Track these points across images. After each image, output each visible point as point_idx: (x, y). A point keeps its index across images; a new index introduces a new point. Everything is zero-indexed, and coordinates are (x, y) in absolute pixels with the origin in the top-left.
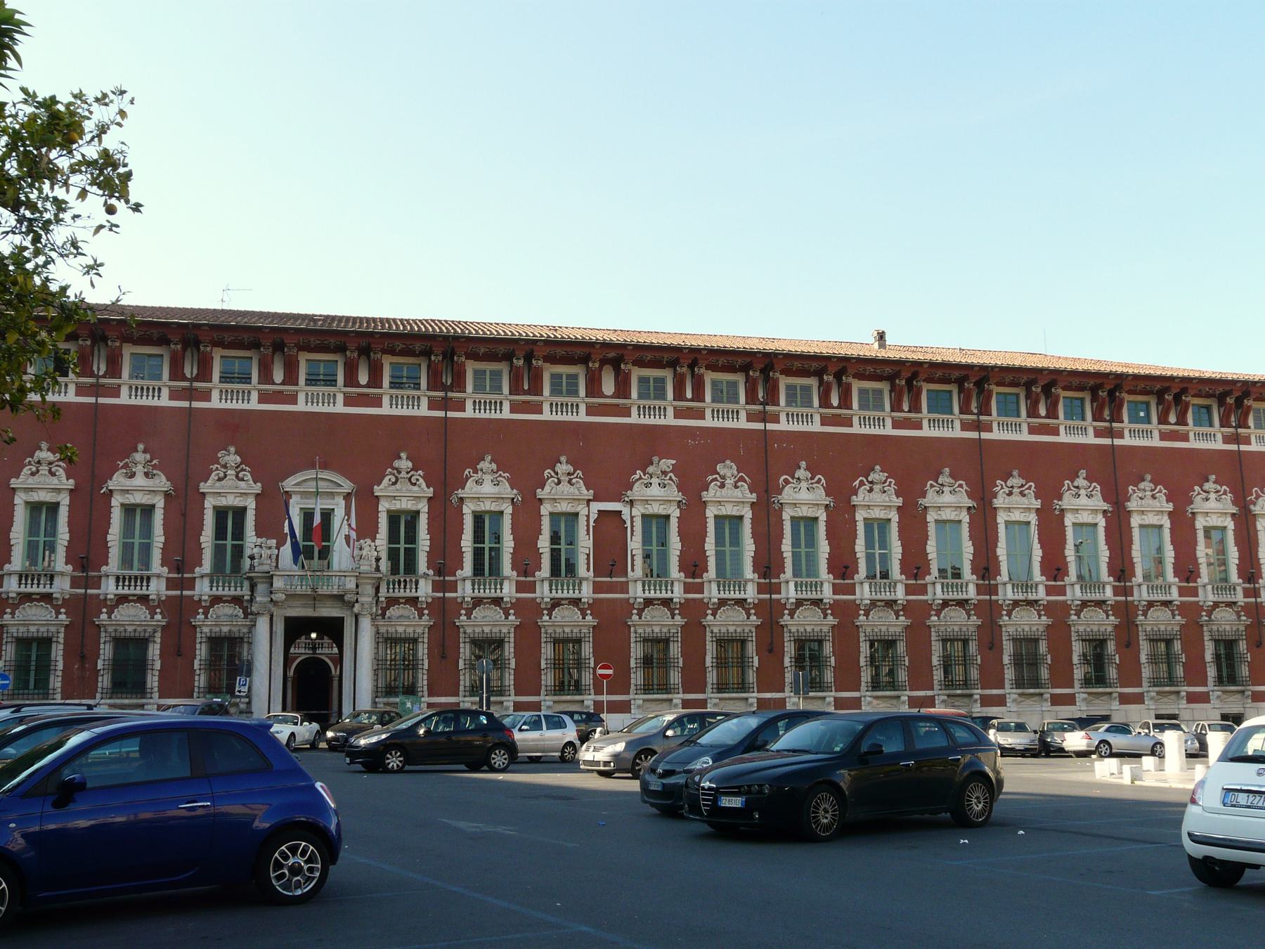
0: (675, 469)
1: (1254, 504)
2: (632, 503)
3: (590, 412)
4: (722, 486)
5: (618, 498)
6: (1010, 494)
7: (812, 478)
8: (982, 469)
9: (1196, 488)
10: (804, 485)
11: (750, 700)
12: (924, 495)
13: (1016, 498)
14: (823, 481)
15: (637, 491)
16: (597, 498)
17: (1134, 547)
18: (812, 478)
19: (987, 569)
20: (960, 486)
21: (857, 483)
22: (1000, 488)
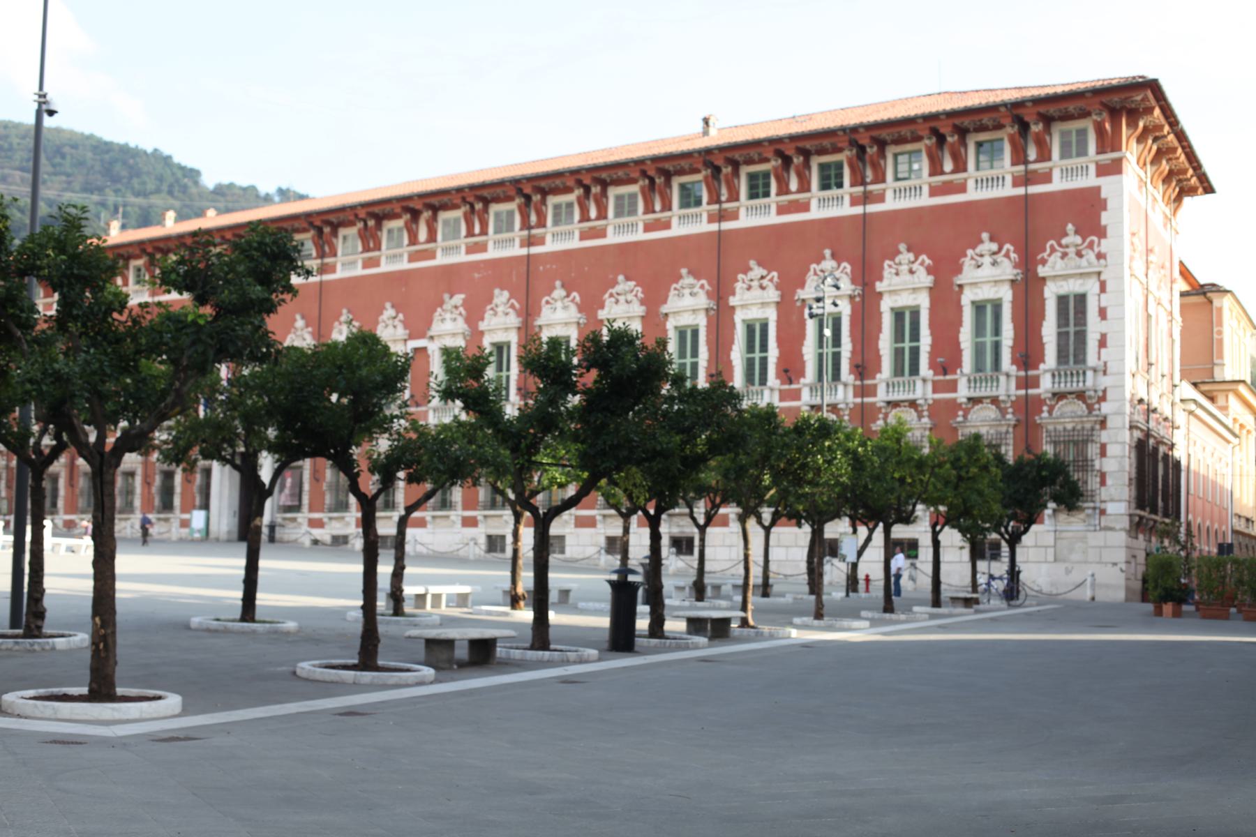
0: (465, 303)
1: (1044, 262)
2: (432, 338)
3: (411, 260)
4: (495, 314)
5: (421, 335)
6: (749, 288)
7: (568, 296)
8: (865, 248)
9: (970, 252)
10: (559, 304)
11: (453, 518)
12: (959, 270)
13: (756, 292)
14: (578, 299)
15: (436, 328)
16: (412, 337)
17: (882, 336)
18: (568, 296)
19: (1027, 356)
20: (702, 287)
21: (607, 296)
22: (888, 269)
